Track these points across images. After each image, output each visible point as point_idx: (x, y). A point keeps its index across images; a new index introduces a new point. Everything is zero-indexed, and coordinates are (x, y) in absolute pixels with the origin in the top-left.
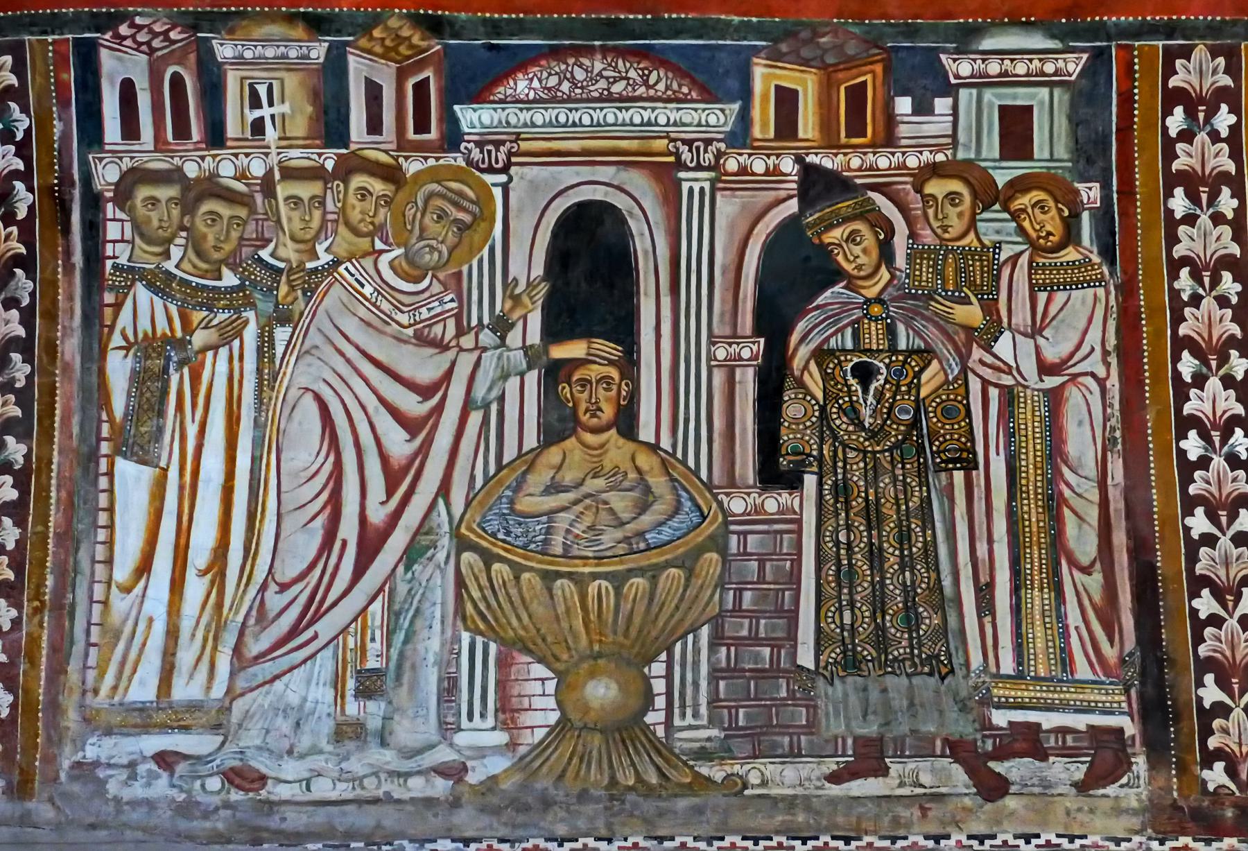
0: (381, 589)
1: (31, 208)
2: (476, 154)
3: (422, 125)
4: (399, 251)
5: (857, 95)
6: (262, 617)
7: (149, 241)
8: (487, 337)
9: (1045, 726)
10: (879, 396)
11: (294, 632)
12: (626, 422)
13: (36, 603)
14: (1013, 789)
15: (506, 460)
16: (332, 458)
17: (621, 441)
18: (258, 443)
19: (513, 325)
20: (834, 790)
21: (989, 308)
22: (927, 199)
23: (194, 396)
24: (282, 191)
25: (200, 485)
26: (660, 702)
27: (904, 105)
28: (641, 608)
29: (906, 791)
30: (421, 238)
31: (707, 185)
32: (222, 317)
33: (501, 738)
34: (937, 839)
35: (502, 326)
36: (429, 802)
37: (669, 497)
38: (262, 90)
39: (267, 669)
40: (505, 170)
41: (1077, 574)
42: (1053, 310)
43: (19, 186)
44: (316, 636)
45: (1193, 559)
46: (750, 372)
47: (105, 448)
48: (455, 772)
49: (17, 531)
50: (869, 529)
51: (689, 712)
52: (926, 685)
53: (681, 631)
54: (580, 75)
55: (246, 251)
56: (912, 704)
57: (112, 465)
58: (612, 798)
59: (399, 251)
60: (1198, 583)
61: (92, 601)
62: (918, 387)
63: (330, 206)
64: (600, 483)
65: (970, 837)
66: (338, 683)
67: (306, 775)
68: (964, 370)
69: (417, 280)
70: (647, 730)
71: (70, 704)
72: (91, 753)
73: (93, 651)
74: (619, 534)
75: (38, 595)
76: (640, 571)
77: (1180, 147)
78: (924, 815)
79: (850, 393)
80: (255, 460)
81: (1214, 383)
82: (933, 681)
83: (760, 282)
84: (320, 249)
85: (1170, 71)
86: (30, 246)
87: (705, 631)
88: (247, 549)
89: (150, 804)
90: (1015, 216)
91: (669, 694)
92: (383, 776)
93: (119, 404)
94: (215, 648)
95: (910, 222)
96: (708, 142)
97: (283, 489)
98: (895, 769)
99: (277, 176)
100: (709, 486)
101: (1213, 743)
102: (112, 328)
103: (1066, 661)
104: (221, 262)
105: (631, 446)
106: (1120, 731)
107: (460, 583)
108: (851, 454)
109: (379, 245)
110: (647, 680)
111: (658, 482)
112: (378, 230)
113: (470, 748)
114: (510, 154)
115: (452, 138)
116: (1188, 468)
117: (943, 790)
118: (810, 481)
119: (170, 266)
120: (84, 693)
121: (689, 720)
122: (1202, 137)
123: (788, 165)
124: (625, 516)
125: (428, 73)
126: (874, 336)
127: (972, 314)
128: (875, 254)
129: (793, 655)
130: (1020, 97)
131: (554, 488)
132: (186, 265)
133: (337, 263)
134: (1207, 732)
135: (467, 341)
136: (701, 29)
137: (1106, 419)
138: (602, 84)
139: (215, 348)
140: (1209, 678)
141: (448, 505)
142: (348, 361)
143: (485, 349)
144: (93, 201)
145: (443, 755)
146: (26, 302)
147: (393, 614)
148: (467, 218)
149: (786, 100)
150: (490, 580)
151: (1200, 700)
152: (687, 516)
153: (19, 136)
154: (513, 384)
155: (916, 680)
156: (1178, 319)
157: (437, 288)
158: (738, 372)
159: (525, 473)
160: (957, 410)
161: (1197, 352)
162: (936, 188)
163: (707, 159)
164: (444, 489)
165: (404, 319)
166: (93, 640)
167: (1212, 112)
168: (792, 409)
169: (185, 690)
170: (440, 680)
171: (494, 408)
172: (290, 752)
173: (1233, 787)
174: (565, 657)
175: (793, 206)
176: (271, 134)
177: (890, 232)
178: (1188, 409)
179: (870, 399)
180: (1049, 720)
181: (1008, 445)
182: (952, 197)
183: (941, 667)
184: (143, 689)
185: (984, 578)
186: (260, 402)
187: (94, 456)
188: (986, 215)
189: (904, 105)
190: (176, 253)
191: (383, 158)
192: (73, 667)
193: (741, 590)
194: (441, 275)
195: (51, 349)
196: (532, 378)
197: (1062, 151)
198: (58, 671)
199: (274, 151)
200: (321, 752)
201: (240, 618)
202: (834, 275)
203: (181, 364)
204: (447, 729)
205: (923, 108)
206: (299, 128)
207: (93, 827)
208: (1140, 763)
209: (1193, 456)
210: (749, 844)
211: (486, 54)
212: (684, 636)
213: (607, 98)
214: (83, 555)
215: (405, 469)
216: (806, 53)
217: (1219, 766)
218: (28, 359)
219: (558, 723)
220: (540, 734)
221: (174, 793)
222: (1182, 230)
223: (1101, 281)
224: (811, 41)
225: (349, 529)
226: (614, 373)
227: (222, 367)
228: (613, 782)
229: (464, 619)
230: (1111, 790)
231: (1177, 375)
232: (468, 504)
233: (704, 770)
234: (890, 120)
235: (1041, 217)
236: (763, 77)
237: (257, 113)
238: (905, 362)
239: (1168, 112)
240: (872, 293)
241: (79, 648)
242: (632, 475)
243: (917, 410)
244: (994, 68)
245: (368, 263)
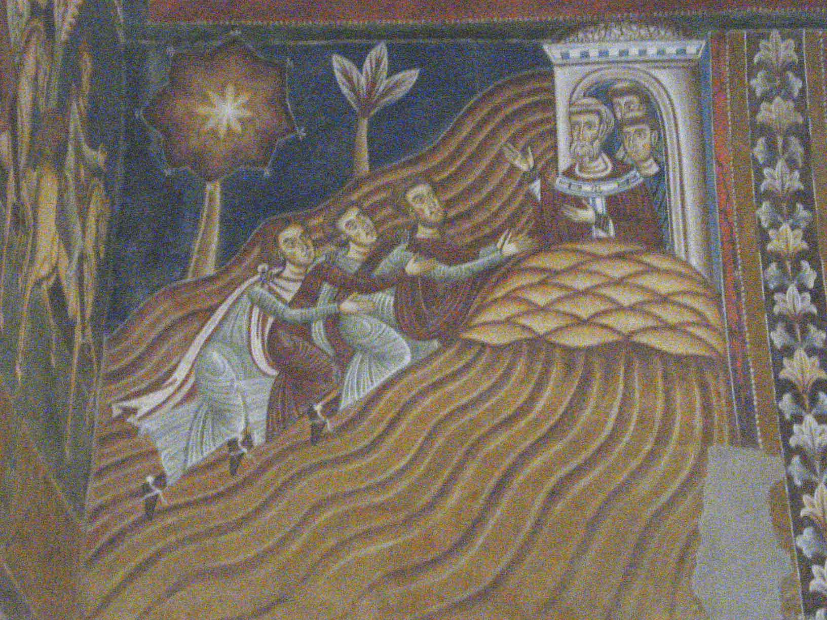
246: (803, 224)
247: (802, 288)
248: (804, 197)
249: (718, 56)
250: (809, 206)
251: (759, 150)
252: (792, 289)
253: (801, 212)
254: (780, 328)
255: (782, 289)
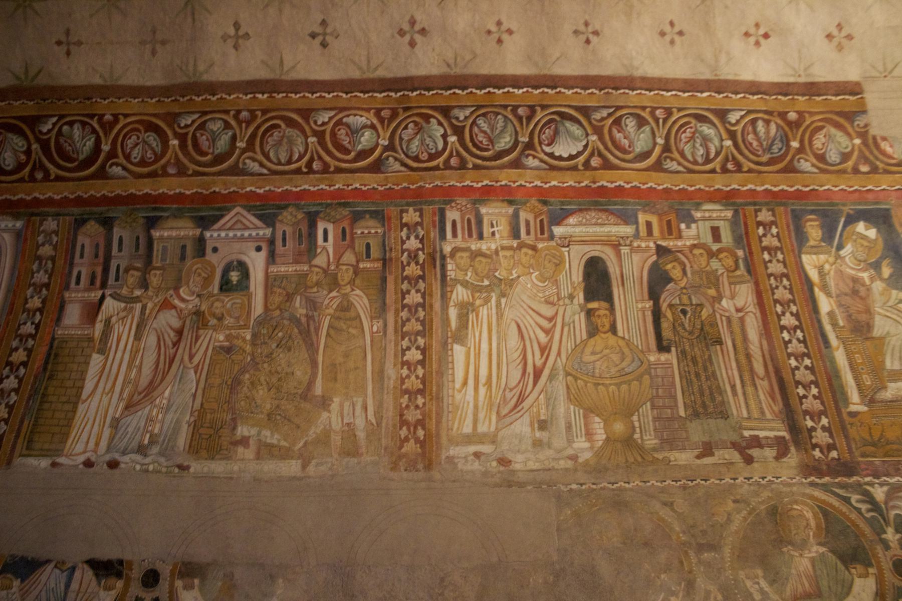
0: (542, 391)
1: (424, 260)
2: (559, 242)
3: (542, 233)
4: (537, 273)
5: (669, 223)
6: (504, 400)
7: (461, 270)
8: (567, 301)
9: (761, 436)
10: (690, 320)
11: (516, 406)
12: (613, 329)
13: (430, 397)
14: (755, 460)
15: (578, 343)
16: (522, 344)
17: (613, 336)
18: (499, 338)
19: (574, 297)
20: (698, 462)
21: (718, 291)
22: (694, 255)
23: (477, 322)
24: (501, 254)
25: (481, 353)
26: (638, 430)
27: (683, 226)
28: (627, 396)
29: (720, 462)
30: (544, 268)
31: (629, 251)
32: (485, 295)
33: (587, 445)
34: (735, 479)
35: (571, 297)
36: (567, 470)
37: (630, 355)
38: (494, 223)
39: (508, 420)
40: (568, 246)
41: (761, 381)
42: (737, 290)
43: (420, 253)
44: (523, 408)
45: (794, 375)
46: (650, 313)
47: (450, 340)
48: (574, 458)
49: (423, 371)
50: (694, 366)
51: (648, 434)
52: (721, 422)
53: (641, 404)
54: (588, 217)
55: (491, 273)
56: (718, 430)
57: (452, 346)
58: (627, 467)
59: (537, 273)
60: (798, 383)
61: (448, 396)
62: (701, 316)
63: (516, 258)
64: (608, 351)
65: (745, 478)
66: (532, 425)
67: (524, 460)
68: (714, 311)
69: (544, 282)
70: (634, 440)
71: (443, 433)
72: (451, 453)
73: (450, 414)
74: (616, 369)
75: (431, 394)
76: (625, 382)
77: (763, 239)
78: (728, 471)
79: (681, 319)
80: (498, 344)
81: (788, 314)
82: (723, 420)
83: (649, 283)
84: (514, 272)
85: (756, 216)
86: (424, 272)
87: (648, 404)
88: (498, 376)
89: (473, 472)
90: (720, 260)
91: (640, 427)
92: (551, 460)
93: (454, 324)
94: (490, 412)
95: (690, 262)
96: (628, 237)
97: (508, 354)
98: (716, 453)
99: (499, 249)
100: (642, 351)
101: (814, 441)
102: (450, 299)
103: (763, 413)
104: (484, 277)
105: (615, 338)
106: (784, 437)
107: (568, 387)
108: (685, 340)
109: (532, 271)
110: (632, 422)
111: (626, 350)
112: (531, 266)
113: (579, 449)
114: (569, 242)
115: (552, 237)
116: (786, 343)
117: (733, 461)
118: (673, 349)
119: (467, 278)
120: (448, 430)
121: (648, 437)
122: (769, 236)
123: (652, 245)
124: (618, 363)
125: (543, 217)
126: (685, 299)
127: (712, 292)
128: (681, 273)
129: (678, 412)
130: (716, 223)
131: (593, 353)
132: (472, 278)
133: (519, 277)
134: (811, 437)
135: (561, 303)
136: (622, 204)
137: (759, 327)
138: (594, 220)
139: (483, 305)
140: (808, 417)
141: (561, 359)
142: (525, 310)
143: (567, 305)
144: (443, 258)
145: (570, 452)
146: (422, 291)
147: (548, 399)
148: (558, 262)
149: (649, 225)
150: (577, 386)
151: (806, 425)
152: (637, 363)
153: (421, 237)
154: (577, 317)
155: (718, 420)
156: (773, 294)
157: (550, 285)
158: (646, 312)
159: (584, 348)
160: (714, 325)
161: (781, 305)
162: (697, 252)
163: (628, 242)
164: (559, 354)
165: (541, 295)
166: (450, 410)
167: (770, 228)
168: (665, 325)
169: (482, 428)
170: (566, 424)
171: (572, 325)
172: (519, 451)
173: (823, 457)
174: (605, 414)
175: (654, 258)
176: (497, 236)
177: (685, 266)
178: (782, 323)
179: (687, 321)
180: (762, 434)
181: (731, 336)
182: (701, 254)
183: (724, 415)
184: (467, 429)
185: (732, 383)
186: (498, 325)
187: (445, 344)
188: (712, 260)
189: (683, 226)
190: (469, 274)
191: (531, 243)
192: (444, 420)
193: (658, 389)
194: (552, 280)
195: (431, 306)
196: (583, 315)
197: (730, 240)
198: (439, 422)
199: (498, 241)
200: (529, 451)
201: (498, 401)
202: (670, 280)
203: (473, 311)
204: (570, 441)
205: (688, 227)
206: (505, 234)
207: (454, 481)
208: (793, 449)
209: (787, 339)
210: (674, 483)
211: (560, 211)
212: (642, 406)
213: (596, 224)
214: (445, 378)
215: (546, 347)
216: (653, 210)
217: (817, 450)
218: (424, 310)
219: (606, 439)
220: (600, 443)
221: (481, 467)
222: (769, 264)
223: (748, 282)
224: (653, 207)
225: (530, 369)
226: (607, 312)
227: (485, 312)
228: (627, 461)
229: (571, 400)
230: (785, 460)
231: (777, 313)
232: (567, 359)
233: (656, 456)
234: (680, 231)
235: (727, 261)
236: (642, 218)
237: (493, 230)
238: (696, 309)
239: (758, 228)
240: (682, 285)
241: (445, 413)
242: (618, 348)
243: (702, 324)
244: (707, 215)
245: (528, 276)
246: (43, 297)
247: (32, 323)
248: (47, 286)
249: (27, 227)
250: (48, 290)
251: (35, 267)
252: (29, 324)
253: (44, 292)
254: (17, 340)
255: (25, 323)
